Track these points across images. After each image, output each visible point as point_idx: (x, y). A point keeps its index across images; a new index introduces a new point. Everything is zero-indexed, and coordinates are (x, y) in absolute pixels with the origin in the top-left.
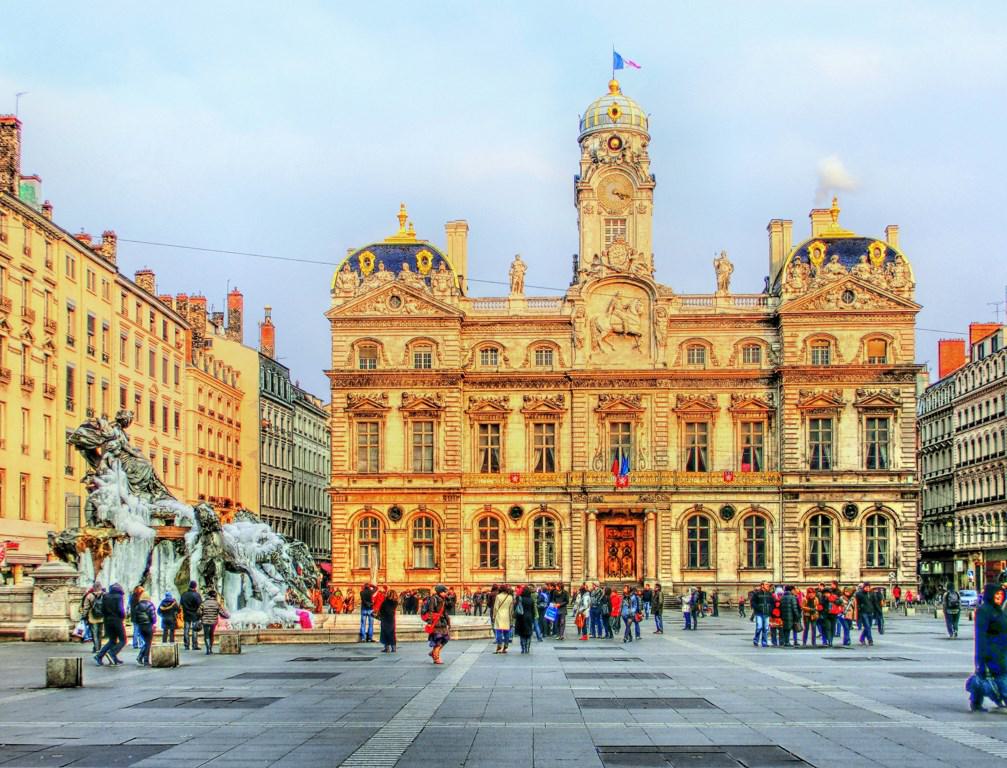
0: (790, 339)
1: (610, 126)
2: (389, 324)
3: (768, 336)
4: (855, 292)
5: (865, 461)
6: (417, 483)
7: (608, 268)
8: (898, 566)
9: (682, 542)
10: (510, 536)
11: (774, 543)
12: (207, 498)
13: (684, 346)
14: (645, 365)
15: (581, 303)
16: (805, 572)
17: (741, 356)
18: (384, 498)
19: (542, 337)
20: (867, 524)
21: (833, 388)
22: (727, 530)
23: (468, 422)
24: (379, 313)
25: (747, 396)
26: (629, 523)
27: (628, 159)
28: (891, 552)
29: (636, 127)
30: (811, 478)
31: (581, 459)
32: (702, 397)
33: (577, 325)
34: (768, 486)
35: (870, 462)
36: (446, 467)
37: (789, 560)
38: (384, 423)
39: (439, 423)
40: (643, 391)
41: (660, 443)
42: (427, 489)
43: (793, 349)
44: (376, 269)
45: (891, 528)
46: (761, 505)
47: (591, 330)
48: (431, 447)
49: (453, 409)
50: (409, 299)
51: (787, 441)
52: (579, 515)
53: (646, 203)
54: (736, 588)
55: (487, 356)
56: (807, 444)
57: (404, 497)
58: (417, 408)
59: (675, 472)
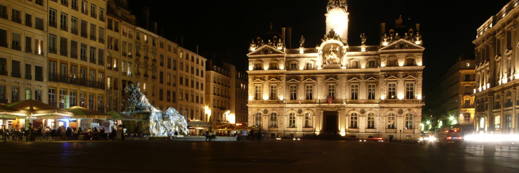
37: (381, 126)
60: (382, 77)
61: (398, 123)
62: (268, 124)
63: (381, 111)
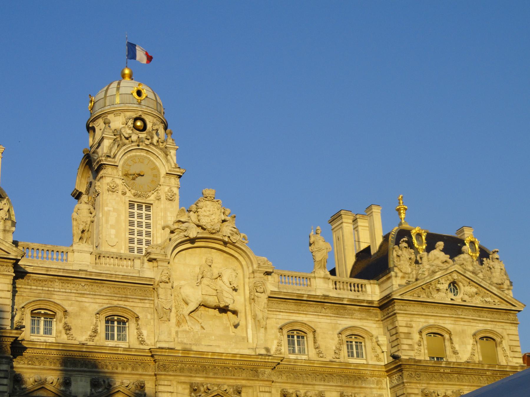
0: (405, 330)
4: (460, 284)
13: (285, 331)
19: (116, 303)
33: (161, 291)
40: (244, 382)
43: (409, 342)
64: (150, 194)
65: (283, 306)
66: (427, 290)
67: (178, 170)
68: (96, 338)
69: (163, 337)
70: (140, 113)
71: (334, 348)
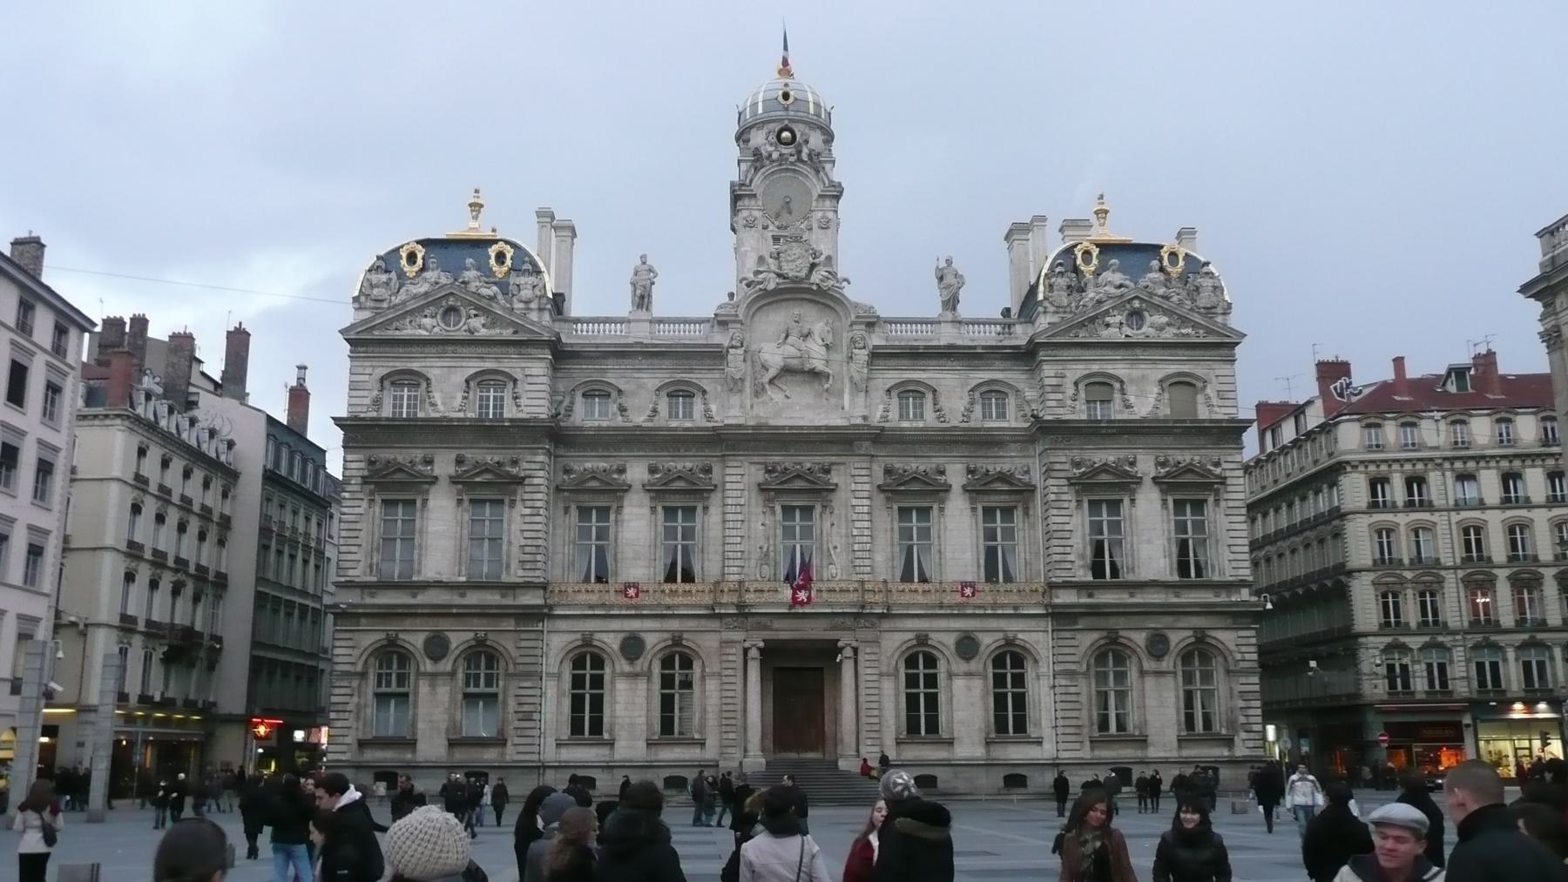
0: (1054, 381)
1: (780, 113)
2: (440, 348)
3: (1013, 376)
4: (1146, 314)
5: (1175, 566)
6: (473, 598)
7: (779, 275)
8: (1237, 732)
9: (897, 695)
10: (621, 685)
11: (1042, 693)
12: (141, 627)
13: (894, 393)
14: (836, 420)
15: (739, 326)
16: (1091, 742)
17: (978, 409)
18: (418, 621)
20: (1183, 665)
21: (1122, 454)
22: (969, 674)
23: (561, 505)
24: (424, 333)
25: (991, 468)
26: (811, 665)
27: (804, 157)
28: (1223, 709)
29: (815, 118)
30: (1096, 592)
31: (738, 563)
32: (922, 468)
34: (1029, 605)
35: (1183, 568)
36: (520, 573)
37: (1068, 722)
38: (425, 501)
39: (513, 503)
40: (834, 459)
41: (858, 539)
42: (490, 607)
43: (1060, 396)
44: (423, 269)
45: (1221, 670)
46: (1020, 636)
47: (753, 366)
48: (495, 541)
49: (536, 481)
50: (473, 312)
51: (1056, 535)
52: (734, 651)
53: (830, 215)
54: (984, 768)
55: (592, 406)
56: (1088, 538)
57: (451, 620)
58: (478, 479)
59: (885, 582)
60: (1057, 467)
61: (1151, 702)
62: (446, 717)
63: (1061, 643)
64: (798, 223)
65: (892, 362)
66: (1091, 326)
67: (832, 189)
68: (657, 418)
69: (735, 412)
70: (786, 122)
71: (963, 409)
